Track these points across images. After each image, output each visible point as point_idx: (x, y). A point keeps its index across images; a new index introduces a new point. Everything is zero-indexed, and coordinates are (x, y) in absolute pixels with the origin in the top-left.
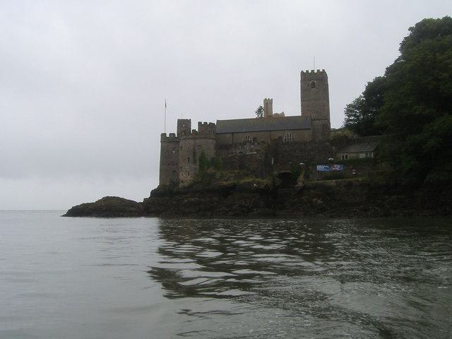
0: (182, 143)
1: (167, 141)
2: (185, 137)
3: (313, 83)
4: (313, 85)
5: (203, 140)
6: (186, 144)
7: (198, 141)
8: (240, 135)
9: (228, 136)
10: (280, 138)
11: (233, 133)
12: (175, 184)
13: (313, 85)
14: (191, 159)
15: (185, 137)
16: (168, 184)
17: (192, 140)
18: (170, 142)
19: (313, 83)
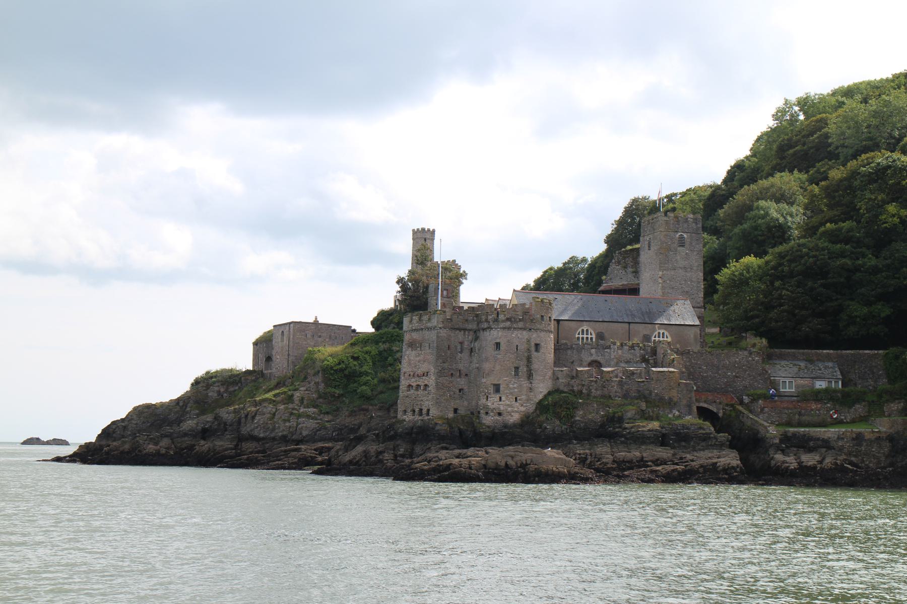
2: (508, 324)
3: (681, 237)
13: (682, 243)
14: (523, 369)
17: (524, 332)
18: (454, 329)
19: (681, 237)
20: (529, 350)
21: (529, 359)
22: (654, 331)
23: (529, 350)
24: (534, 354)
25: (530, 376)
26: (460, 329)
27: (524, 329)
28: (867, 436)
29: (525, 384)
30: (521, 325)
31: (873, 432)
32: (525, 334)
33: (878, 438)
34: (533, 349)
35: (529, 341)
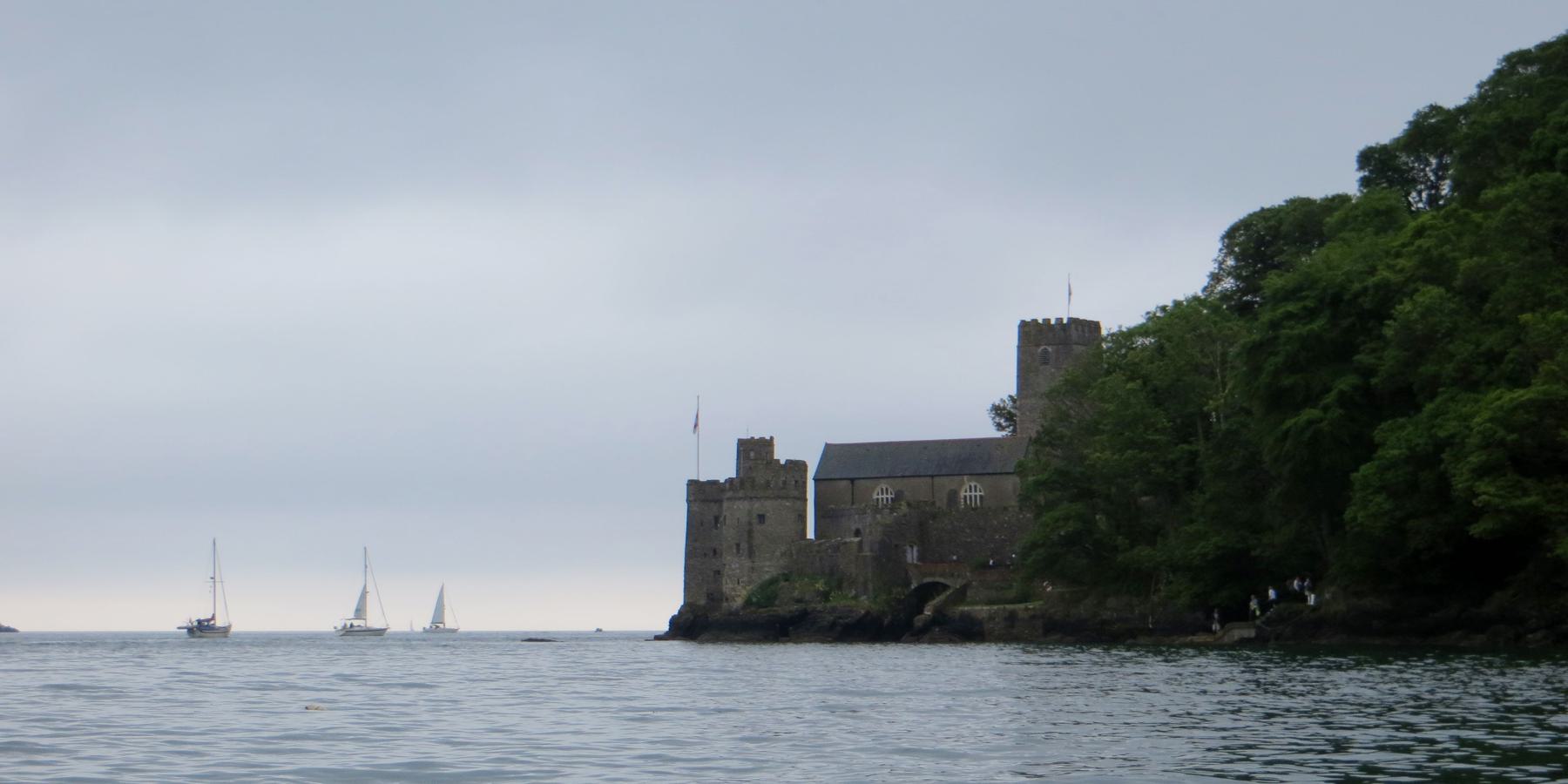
0: (725, 505)
1: (702, 495)
2: (729, 494)
3: (1045, 351)
4: (1045, 359)
5: (768, 503)
6: (737, 511)
7: (757, 505)
8: (868, 483)
9: (844, 483)
10: (953, 496)
11: (852, 480)
12: (715, 598)
13: (1045, 359)
14: (744, 546)
15: (729, 494)
16: (702, 602)
18: (704, 501)
19: (1045, 351)
20: (750, 523)
21: (750, 533)
22: (961, 484)
23: (750, 523)
24: (757, 528)
25: (751, 554)
26: (716, 501)
27: (744, 498)
28: (1021, 615)
29: (747, 563)
30: (741, 494)
31: (1027, 609)
32: (743, 506)
33: (1033, 617)
34: (755, 521)
35: (750, 512)
